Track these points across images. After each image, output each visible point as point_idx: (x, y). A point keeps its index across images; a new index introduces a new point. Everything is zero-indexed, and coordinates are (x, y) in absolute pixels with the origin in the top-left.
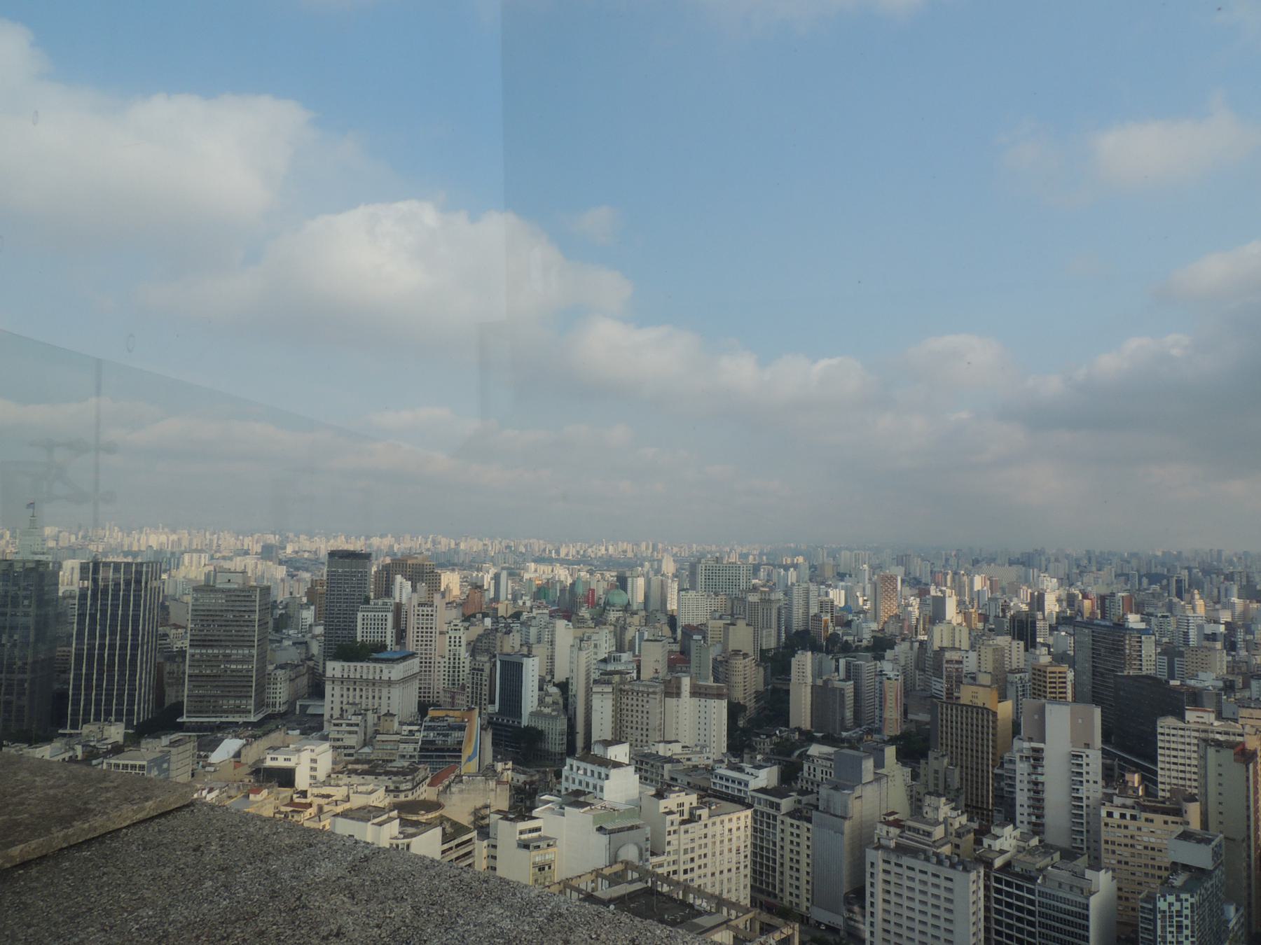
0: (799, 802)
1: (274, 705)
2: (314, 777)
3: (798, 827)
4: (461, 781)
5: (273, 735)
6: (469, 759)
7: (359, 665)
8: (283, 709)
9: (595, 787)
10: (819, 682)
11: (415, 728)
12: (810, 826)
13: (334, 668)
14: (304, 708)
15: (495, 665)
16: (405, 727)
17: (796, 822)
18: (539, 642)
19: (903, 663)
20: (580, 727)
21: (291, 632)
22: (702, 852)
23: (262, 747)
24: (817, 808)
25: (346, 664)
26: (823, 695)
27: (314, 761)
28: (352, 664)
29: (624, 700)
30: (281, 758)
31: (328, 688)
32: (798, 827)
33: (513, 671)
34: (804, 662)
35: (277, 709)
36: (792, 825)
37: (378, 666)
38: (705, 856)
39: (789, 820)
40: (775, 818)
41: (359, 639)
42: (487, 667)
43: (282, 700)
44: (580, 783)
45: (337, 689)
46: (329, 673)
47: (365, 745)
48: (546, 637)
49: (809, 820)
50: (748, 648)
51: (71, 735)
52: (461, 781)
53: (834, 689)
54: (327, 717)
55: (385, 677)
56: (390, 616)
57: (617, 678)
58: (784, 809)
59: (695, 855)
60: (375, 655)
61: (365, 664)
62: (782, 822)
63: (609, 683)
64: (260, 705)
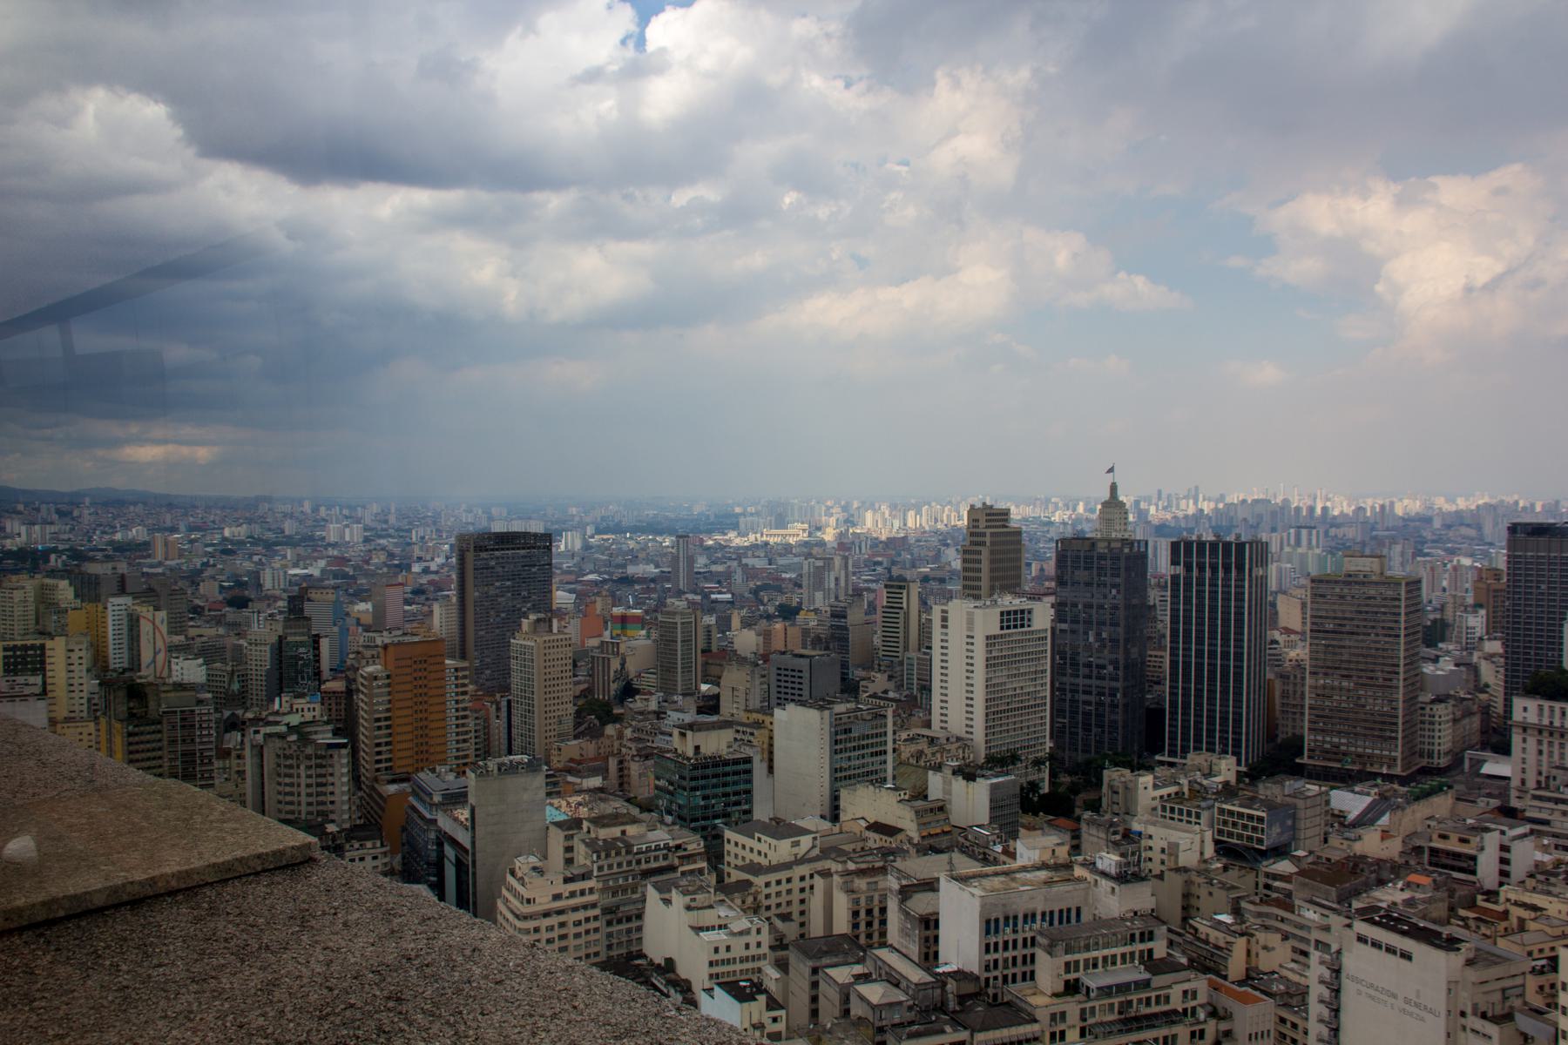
1: (1430, 755)
8: (1443, 762)
13: (1527, 709)
21: (1451, 647)
23: (1419, 815)
25: (1546, 704)
27: (1504, 848)
28: (1557, 705)
30: (1454, 837)
31: (1516, 739)
35: (1436, 761)
45: (1532, 743)
46: (1517, 715)
51: (1172, 765)
54: (1515, 783)
64: (1412, 752)
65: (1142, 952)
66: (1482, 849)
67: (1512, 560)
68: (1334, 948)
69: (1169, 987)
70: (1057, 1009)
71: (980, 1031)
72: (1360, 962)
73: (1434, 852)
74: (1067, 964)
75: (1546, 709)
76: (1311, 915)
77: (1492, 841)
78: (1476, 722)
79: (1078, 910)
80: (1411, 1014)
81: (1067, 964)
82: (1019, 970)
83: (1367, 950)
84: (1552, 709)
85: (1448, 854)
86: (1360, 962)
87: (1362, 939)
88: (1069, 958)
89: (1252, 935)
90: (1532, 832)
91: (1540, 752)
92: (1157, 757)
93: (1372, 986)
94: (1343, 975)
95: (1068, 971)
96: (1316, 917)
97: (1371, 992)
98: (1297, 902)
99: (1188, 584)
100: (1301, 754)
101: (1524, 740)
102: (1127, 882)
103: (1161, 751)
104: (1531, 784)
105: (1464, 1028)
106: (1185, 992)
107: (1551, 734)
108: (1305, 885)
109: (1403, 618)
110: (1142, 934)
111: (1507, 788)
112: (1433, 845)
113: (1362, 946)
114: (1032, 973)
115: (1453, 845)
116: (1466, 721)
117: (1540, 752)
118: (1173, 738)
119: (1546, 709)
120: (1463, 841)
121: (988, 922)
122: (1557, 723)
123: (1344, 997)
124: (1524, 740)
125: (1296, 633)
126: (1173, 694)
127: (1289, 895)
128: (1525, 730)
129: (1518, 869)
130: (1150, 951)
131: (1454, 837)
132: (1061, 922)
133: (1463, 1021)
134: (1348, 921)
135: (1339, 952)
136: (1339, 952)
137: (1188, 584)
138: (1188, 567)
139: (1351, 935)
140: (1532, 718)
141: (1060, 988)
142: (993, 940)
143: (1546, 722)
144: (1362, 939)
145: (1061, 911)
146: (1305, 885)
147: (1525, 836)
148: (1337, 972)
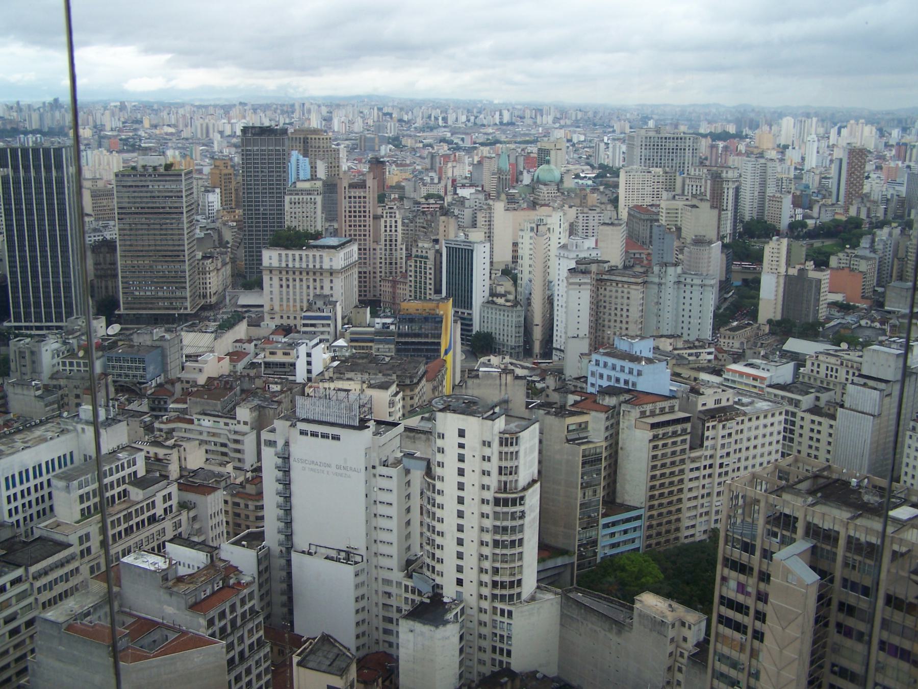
0: (818, 399)
1: (205, 296)
2: (309, 371)
3: (820, 423)
4: (477, 376)
5: (237, 328)
6: (446, 353)
7: (297, 253)
8: (214, 300)
9: (626, 382)
10: (793, 272)
11: (389, 321)
12: (832, 422)
13: (271, 257)
14: (235, 297)
15: (439, 253)
16: (378, 320)
17: (817, 419)
18: (474, 225)
19: (880, 254)
20: (538, 318)
22: (738, 447)
24: (842, 406)
25: (284, 253)
26: (796, 289)
27: (309, 355)
28: (290, 253)
29: (601, 291)
30: (280, 352)
31: (266, 278)
32: (820, 423)
33: (461, 259)
34: (775, 251)
36: (813, 422)
37: (318, 254)
38: (740, 450)
39: (808, 417)
40: (794, 415)
41: (287, 224)
42: (431, 255)
43: (213, 291)
44: (609, 378)
46: (266, 262)
47: (336, 339)
48: (481, 219)
49: (833, 417)
50: (712, 234)
52: (477, 376)
53: (811, 281)
54: (266, 308)
55: (326, 266)
56: (319, 199)
57: (594, 268)
58: (804, 406)
59: (731, 450)
60: (312, 242)
61: (304, 253)
62: (802, 419)
63: (585, 272)
65: (130, 475)
66: (298, 357)
67: (246, 155)
68: (280, 443)
69: (154, 495)
70: (82, 532)
71: (31, 565)
72: (304, 449)
73: (268, 365)
74: (81, 497)
75: (284, 256)
76: (207, 423)
77: (302, 350)
78: (228, 269)
79: (71, 453)
80: (341, 475)
81: (81, 497)
82: (34, 510)
83: (309, 438)
84: (287, 255)
85: (276, 364)
86: (304, 449)
87: (303, 433)
88: (81, 492)
89: (180, 446)
90: (321, 341)
91: (281, 286)
92: (6, 324)
93: (313, 462)
94: (291, 460)
95: (82, 502)
96: (210, 424)
97: (312, 466)
98: (195, 417)
99: (17, 182)
100: (118, 307)
101: (271, 279)
102: (110, 425)
103: (7, 316)
104: (277, 308)
105: (375, 475)
106: (164, 496)
107: (314, 273)
108: (196, 403)
109: (184, 199)
110: (128, 462)
111: (262, 312)
112: (267, 360)
113: (303, 437)
114: (51, 507)
115: (279, 358)
116: (224, 269)
117: (281, 286)
118: (16, 305)
119: (284, 256)
120: (285, 354)
121: (7, 479)
122: (291, 265)
123: (293, 474)
124: (271, 279)
125: (91, 215)
126: (13, 273)
127: (184, 412)
128: (271, 272)
129: (317, 368)
130: (135, 473)
131: (280, 352)
132: (60, 467)
133: (374, 471)
134: (289, 423)
135: (287, 444)
136: (287, 444)
137: (17, 182)
138: (15, 169)
139: (295, 433)
140: (275, 263)
141: (79, 517)
142: (12, 492)
143: (284, 265)
144: (303, 433)
145: (59, 458)
146: (196, 403)
147: (317, 344)
148: (286, 458)
